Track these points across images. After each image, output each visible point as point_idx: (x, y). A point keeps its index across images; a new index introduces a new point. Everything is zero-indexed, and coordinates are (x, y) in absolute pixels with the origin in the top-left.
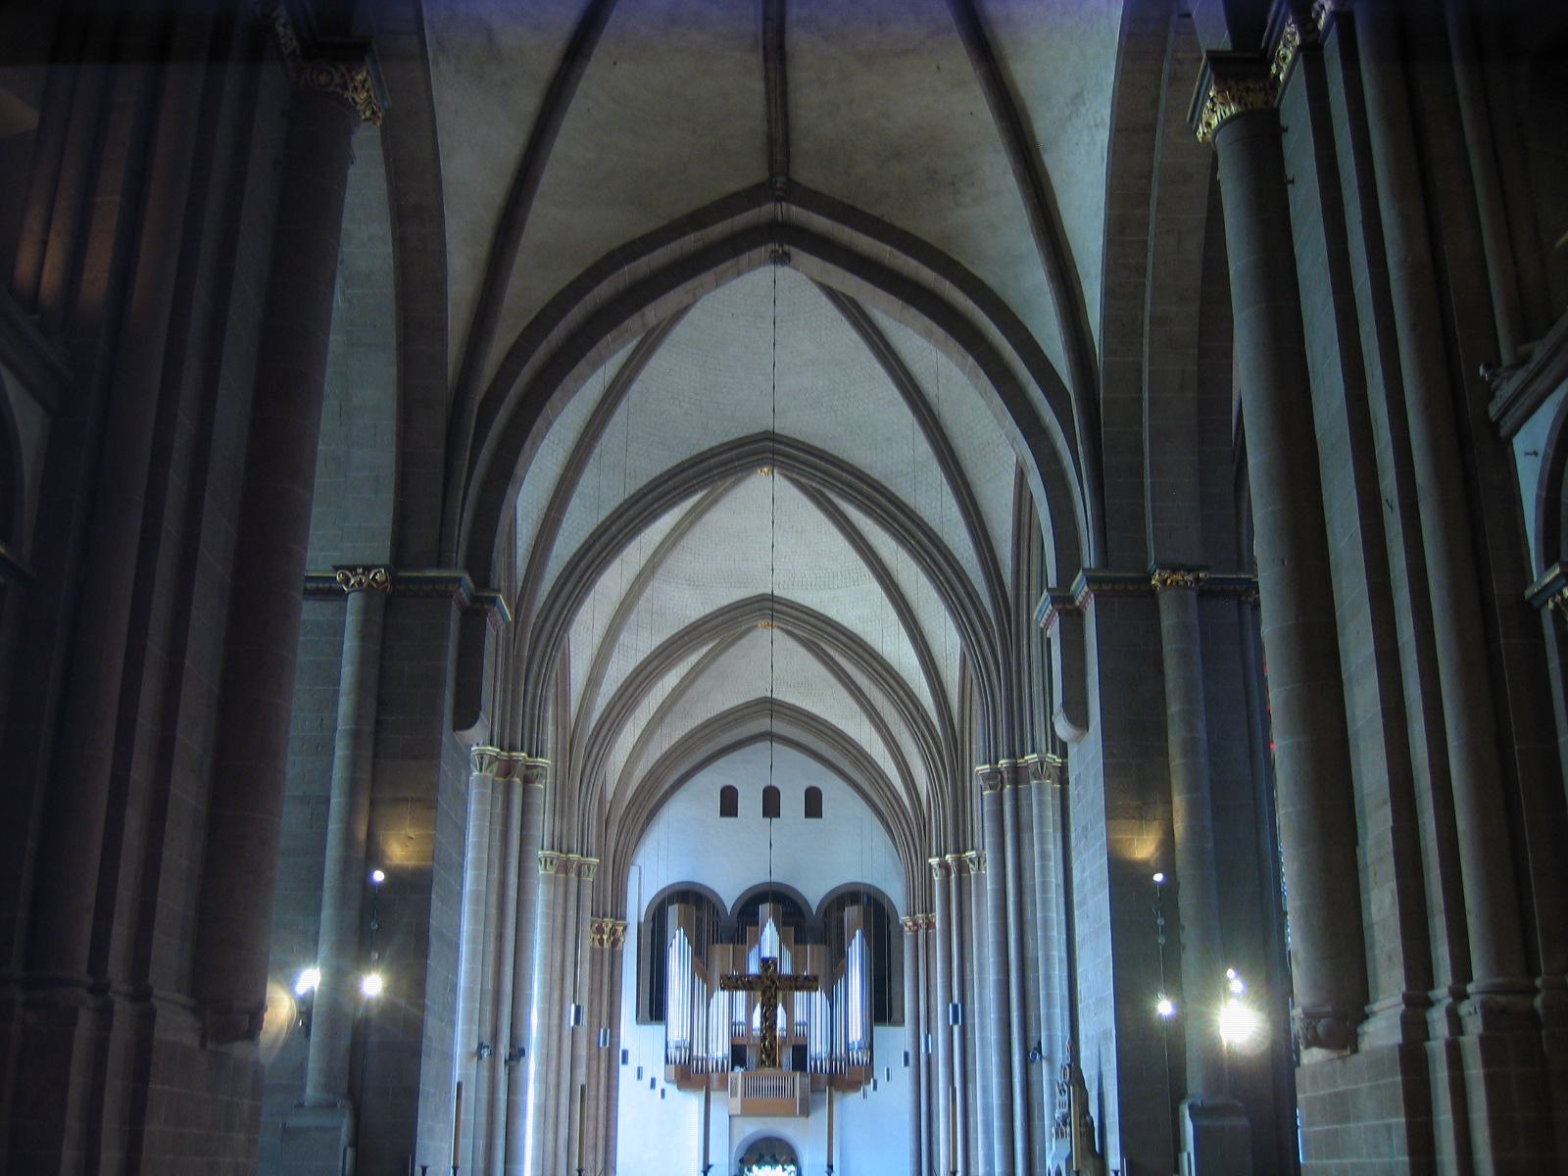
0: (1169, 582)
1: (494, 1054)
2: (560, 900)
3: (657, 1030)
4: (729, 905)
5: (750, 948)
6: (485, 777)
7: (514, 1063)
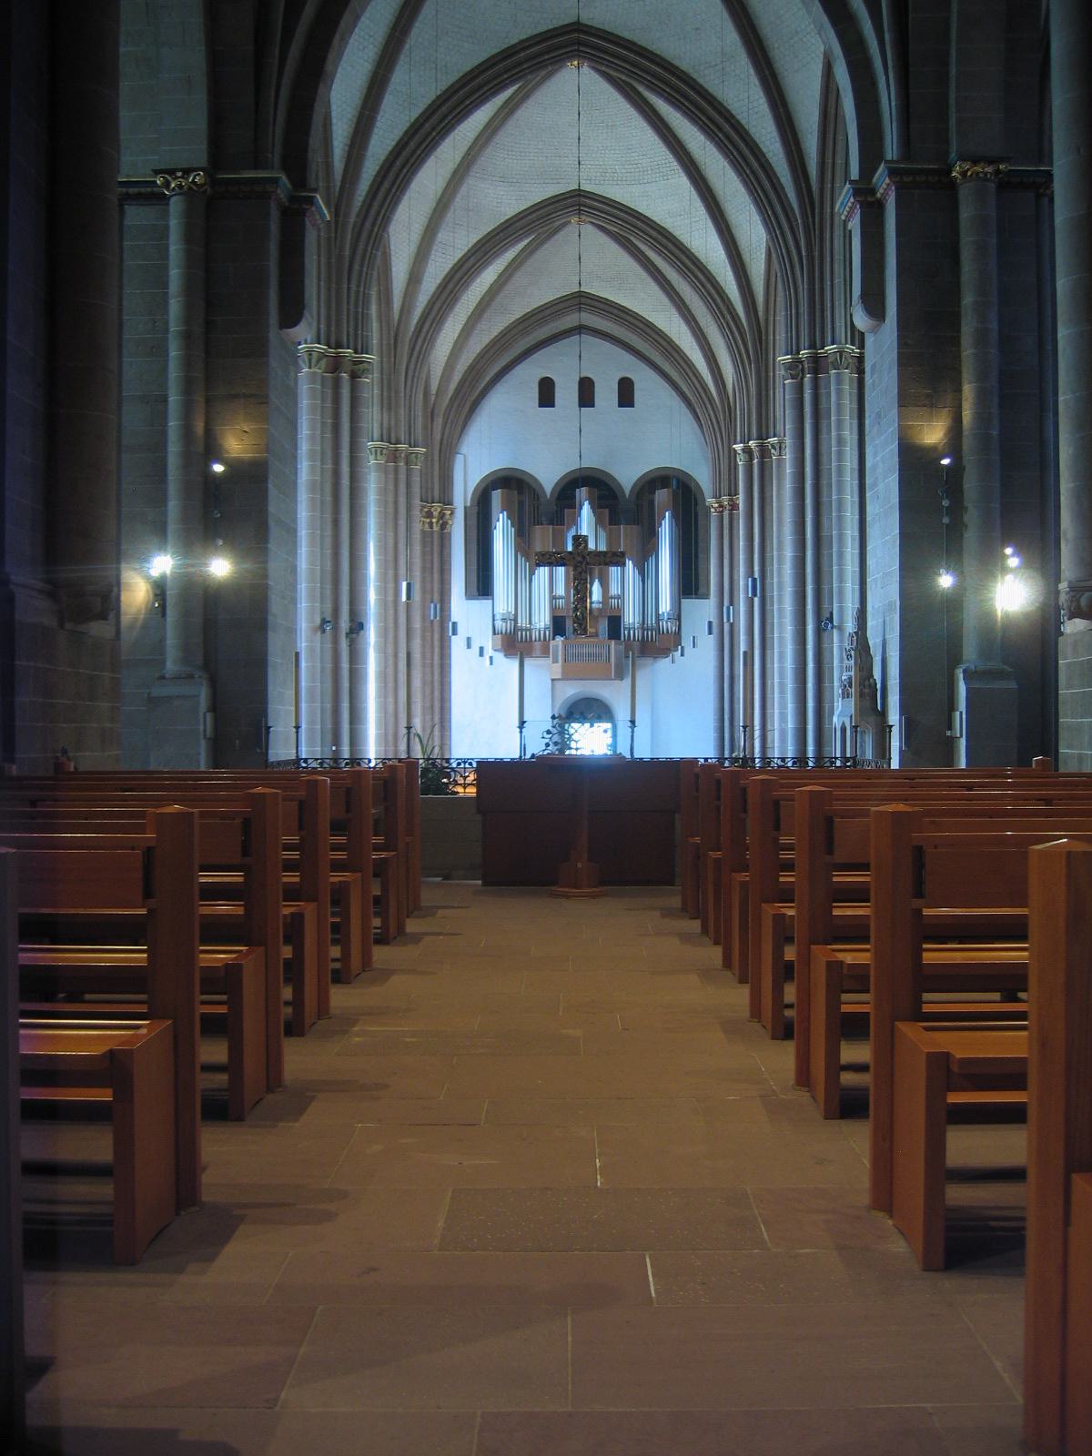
0: (969, 173)
1: (336, 629)
2: (391, 487)
3: (486, 603)
5: (569, 529)
6: (315, 373)
7: (354, 636)
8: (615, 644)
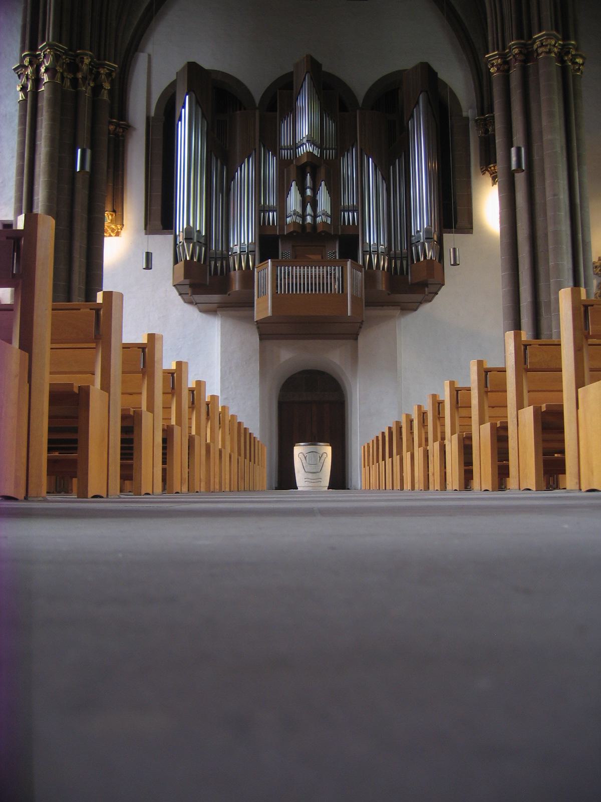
4: (257, 98)
5: (283, 118)
8: (352, 267)
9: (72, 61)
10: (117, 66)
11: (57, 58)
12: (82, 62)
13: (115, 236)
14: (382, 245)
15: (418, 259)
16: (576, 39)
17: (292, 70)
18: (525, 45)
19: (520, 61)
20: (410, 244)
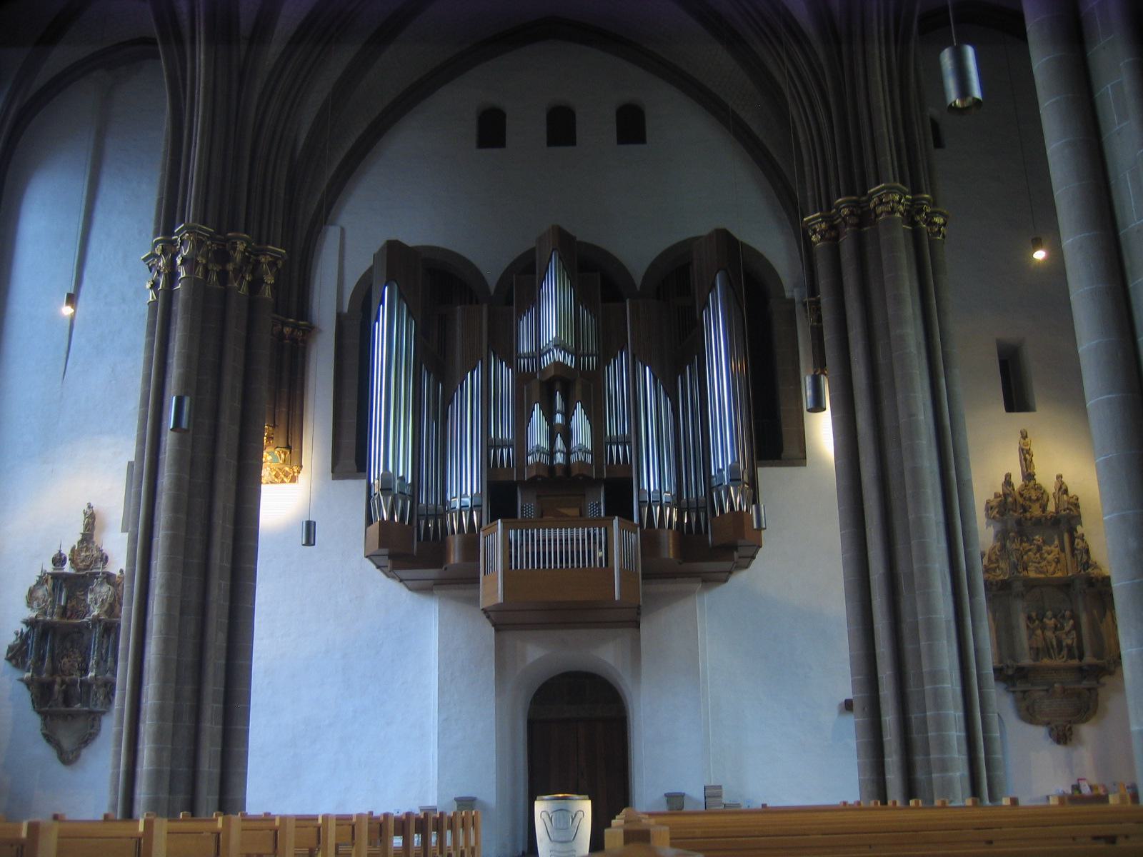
9: (221, 247)
10: (284, 251)
11: (199, 244)
12: (235, 249)
13: (290, 482)
14: (668, 492)
15: (722, 510)
16: (933, 194)
17: (534, 245)
18: (857, 203)
19: (852, 225)
20: (709, 489)
